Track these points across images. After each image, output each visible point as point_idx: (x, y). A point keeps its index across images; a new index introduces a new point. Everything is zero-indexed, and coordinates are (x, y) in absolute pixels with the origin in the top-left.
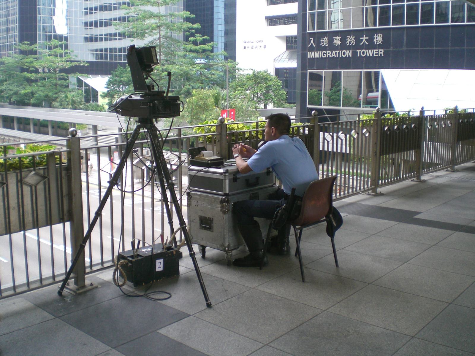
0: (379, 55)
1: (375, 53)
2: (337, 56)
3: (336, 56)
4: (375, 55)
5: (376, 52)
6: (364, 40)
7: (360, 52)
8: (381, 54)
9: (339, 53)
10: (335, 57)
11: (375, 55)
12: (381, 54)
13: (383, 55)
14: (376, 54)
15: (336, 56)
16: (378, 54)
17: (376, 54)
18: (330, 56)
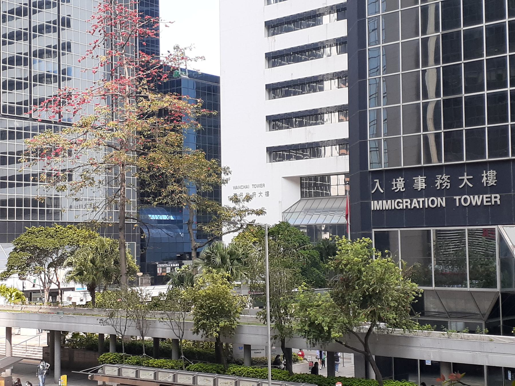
0: (493, 203)
1: (485, 200)
2: (421, 207)
3: (419, 205)
4: (485, 203)
5: (487, 198)
6: (466, 180)
7: (460, 199)
8: (495, 202)
9: (424, 202)
10: (418, 207)
11: (485, 203)
12: (495, 202)
13: (499, 203)
14: (487, 202)
15: (419, 205)
16: (491, 201)
17: (487, 202)
18: (409, 207)
